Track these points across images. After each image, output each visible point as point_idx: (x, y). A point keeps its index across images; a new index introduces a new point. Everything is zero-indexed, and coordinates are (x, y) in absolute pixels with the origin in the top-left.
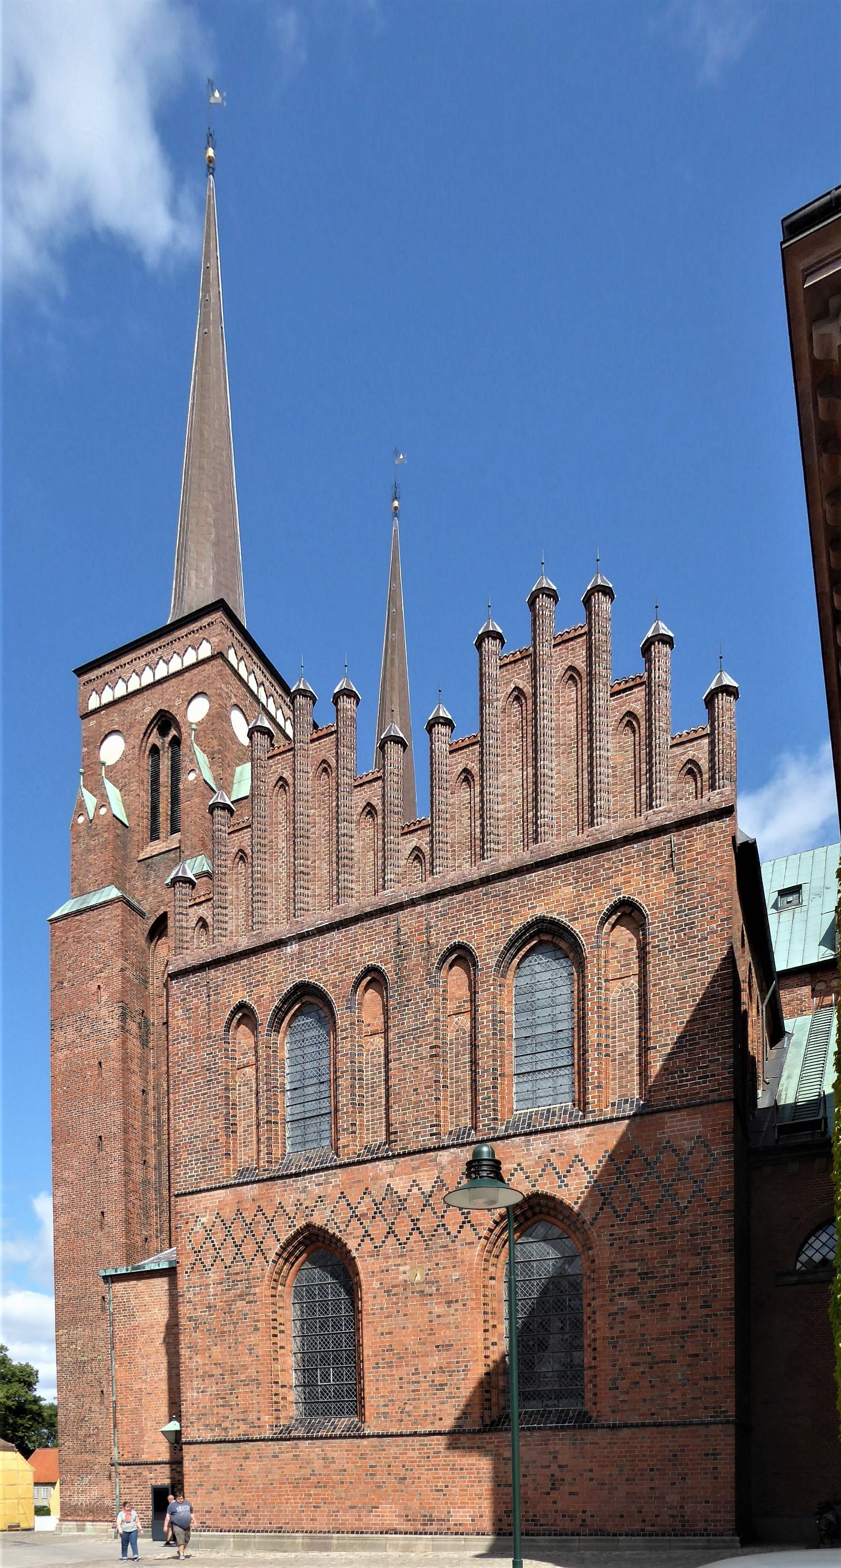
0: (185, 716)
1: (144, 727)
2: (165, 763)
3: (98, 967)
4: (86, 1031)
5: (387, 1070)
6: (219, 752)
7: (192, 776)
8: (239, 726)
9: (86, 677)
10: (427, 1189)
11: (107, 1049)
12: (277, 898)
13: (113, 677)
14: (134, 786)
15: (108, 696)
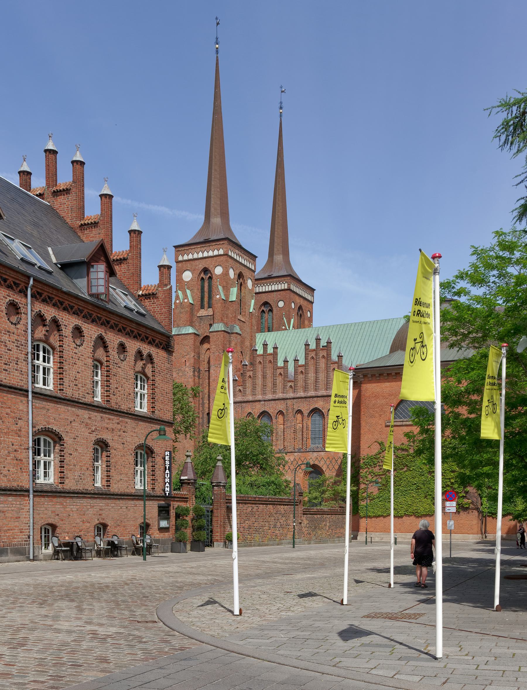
0: (214, 272)
1: (199, 271)
2: (206, 284)
3: (185, 354)
4: (181, 374)
5: (284, 434)
6: (226, 287)
7: (218, 297)
8: (232, 274)
9: (178, 249)
10: (292, 460)
11: (188, 381)
12: (259, 388)
13: (187, 252)
14: (196, 291)
15: (186, 257)
